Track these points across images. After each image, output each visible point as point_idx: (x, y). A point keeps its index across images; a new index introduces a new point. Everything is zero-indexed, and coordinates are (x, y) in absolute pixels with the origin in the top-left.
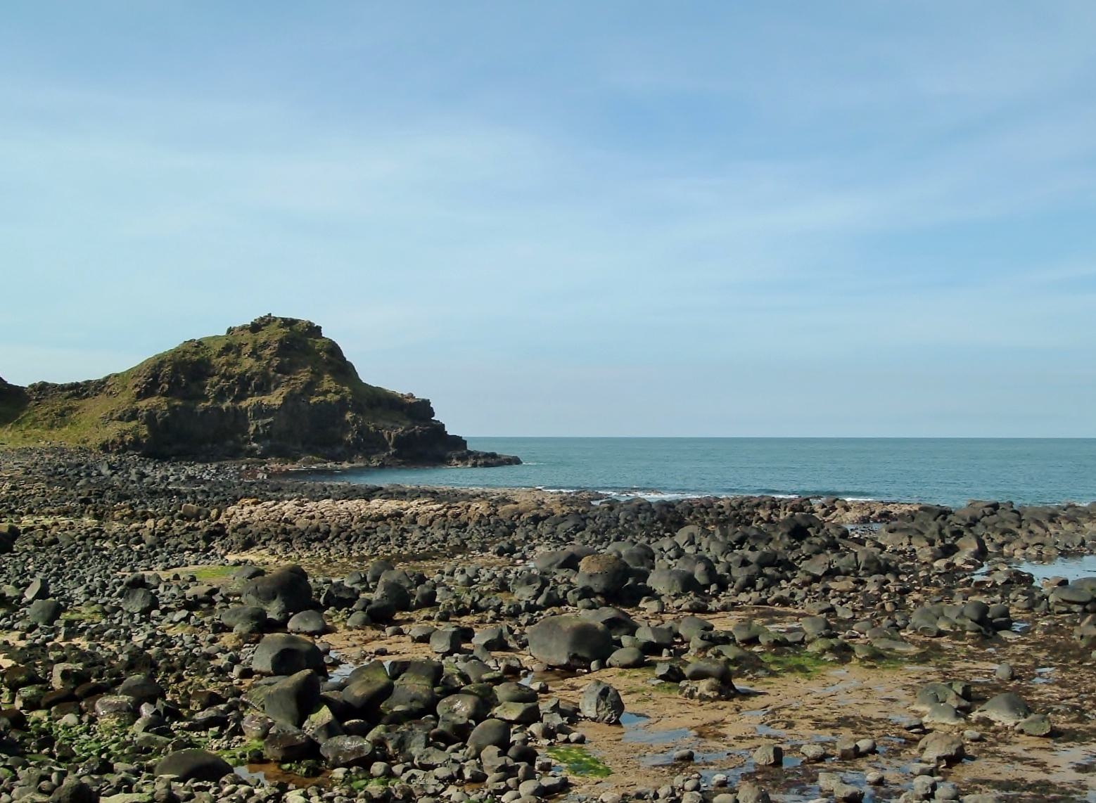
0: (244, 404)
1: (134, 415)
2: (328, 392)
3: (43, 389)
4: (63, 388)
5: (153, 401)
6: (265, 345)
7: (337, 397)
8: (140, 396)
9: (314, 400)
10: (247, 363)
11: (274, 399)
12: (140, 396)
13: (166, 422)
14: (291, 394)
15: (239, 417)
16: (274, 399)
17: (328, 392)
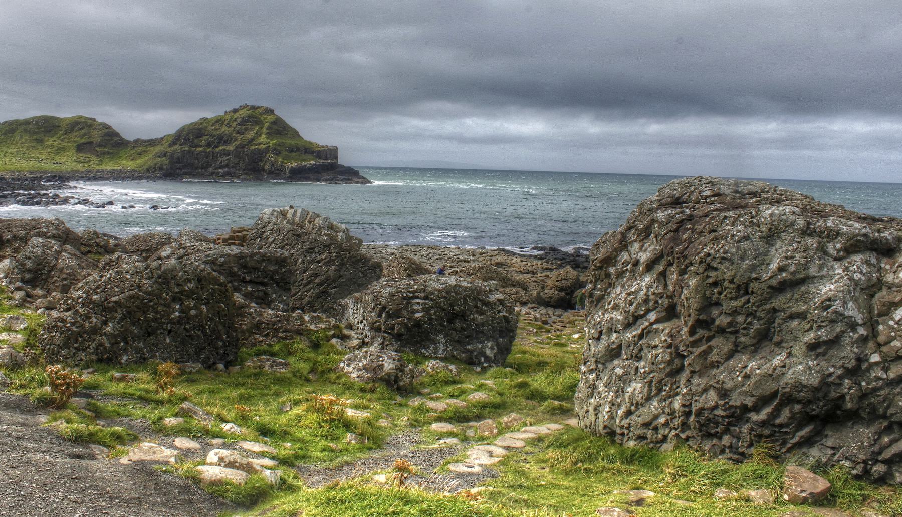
0: (217, 150)
1: (165, 155)
2: (260, 144)
3: (137, 141)
4: (145, 141)
5: (177, 147)
6: (235, 120)
8: (170, 146)
9: (253, 148)
10: (225, 129)
11: (231, 148)
12: (170, 146)
13: (178, 158)
14: (240, 144)
15: (215, 156)
16: (231, 148)
17: (260, 144)
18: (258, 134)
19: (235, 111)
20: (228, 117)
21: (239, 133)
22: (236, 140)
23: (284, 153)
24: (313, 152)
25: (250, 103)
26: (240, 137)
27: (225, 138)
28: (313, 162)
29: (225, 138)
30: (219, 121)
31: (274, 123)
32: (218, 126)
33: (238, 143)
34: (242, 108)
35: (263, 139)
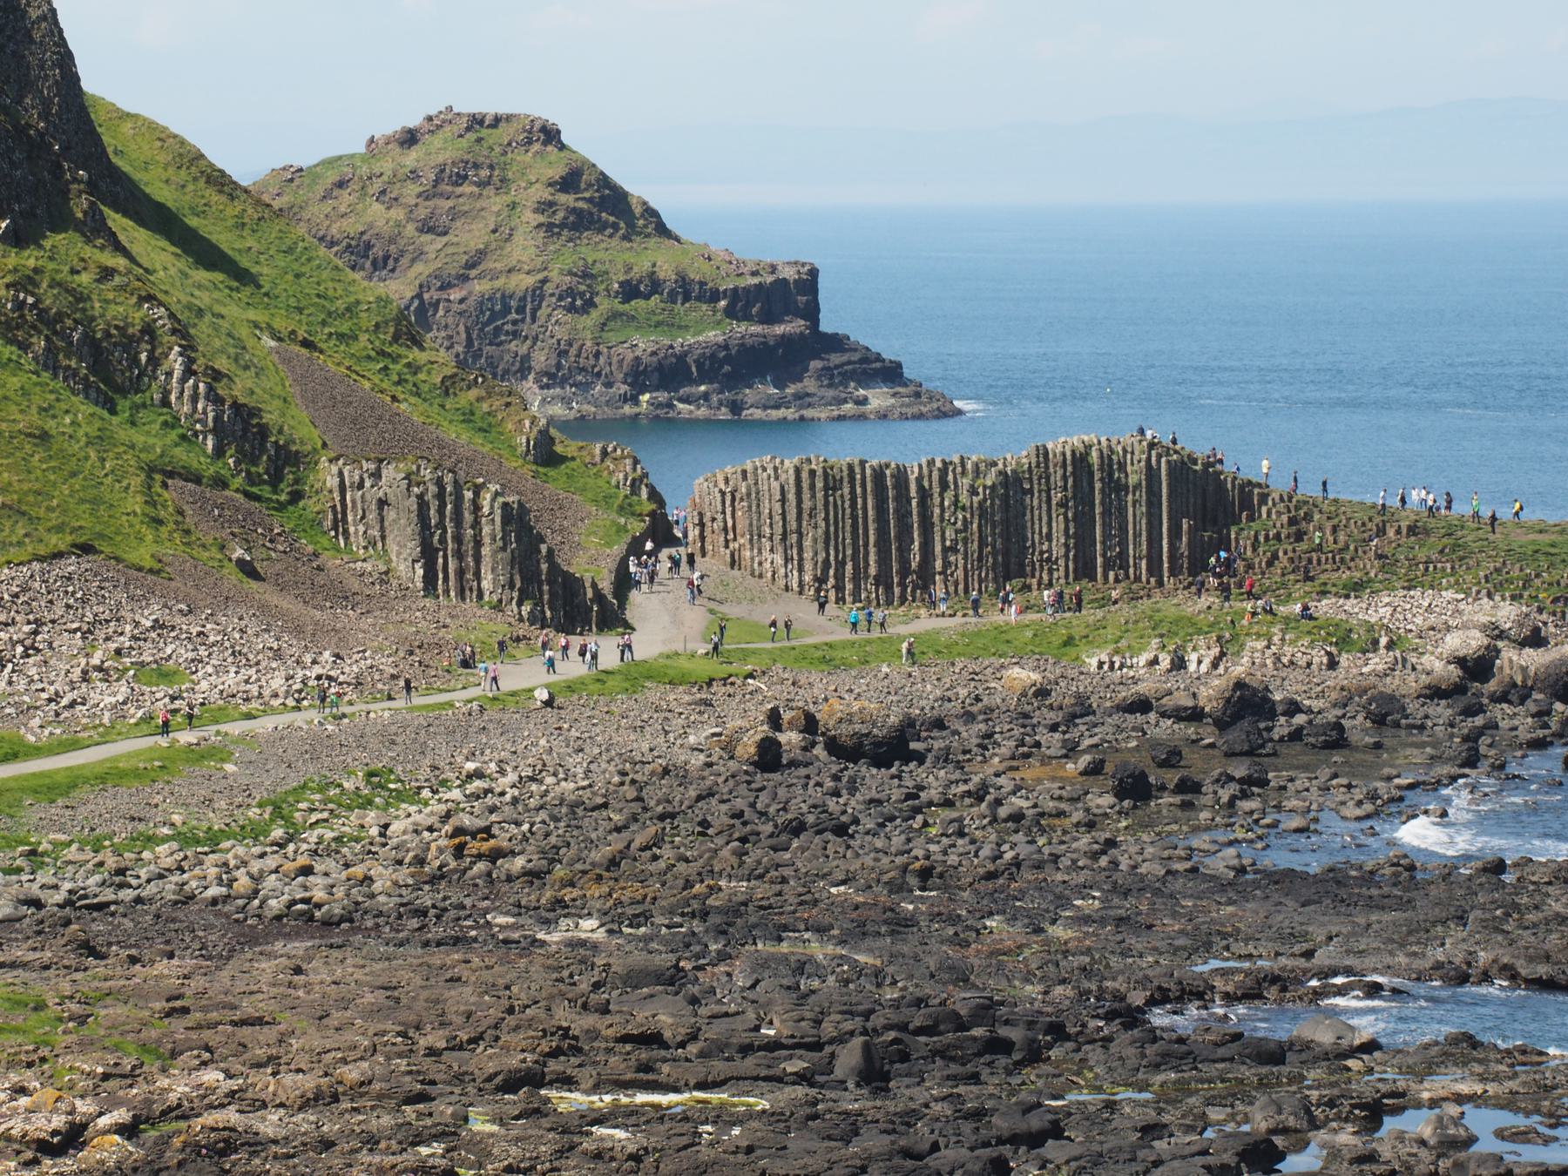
6: (414, 175)
7: (530, 281)
9: (480, 287)
18: (503, 234)
19: (410, 138)
20: (386, 166)
21: (427, 228)
22: (419, 255)
23: (604, 304)
24: (715, 296)
25: (468, 105)
26: (432, 244)
27: (378, 251)
28: (713, 335)
29: (378, 251)
30: (341, 178)
31: (570, 182)
32: (346, 198)
33: (421, 270)
34: (435, 124)
35: (524, 247)
